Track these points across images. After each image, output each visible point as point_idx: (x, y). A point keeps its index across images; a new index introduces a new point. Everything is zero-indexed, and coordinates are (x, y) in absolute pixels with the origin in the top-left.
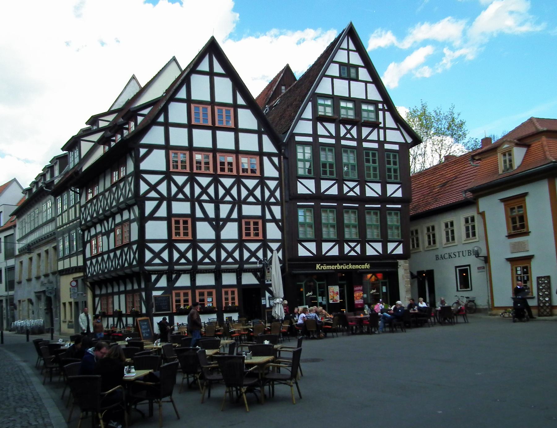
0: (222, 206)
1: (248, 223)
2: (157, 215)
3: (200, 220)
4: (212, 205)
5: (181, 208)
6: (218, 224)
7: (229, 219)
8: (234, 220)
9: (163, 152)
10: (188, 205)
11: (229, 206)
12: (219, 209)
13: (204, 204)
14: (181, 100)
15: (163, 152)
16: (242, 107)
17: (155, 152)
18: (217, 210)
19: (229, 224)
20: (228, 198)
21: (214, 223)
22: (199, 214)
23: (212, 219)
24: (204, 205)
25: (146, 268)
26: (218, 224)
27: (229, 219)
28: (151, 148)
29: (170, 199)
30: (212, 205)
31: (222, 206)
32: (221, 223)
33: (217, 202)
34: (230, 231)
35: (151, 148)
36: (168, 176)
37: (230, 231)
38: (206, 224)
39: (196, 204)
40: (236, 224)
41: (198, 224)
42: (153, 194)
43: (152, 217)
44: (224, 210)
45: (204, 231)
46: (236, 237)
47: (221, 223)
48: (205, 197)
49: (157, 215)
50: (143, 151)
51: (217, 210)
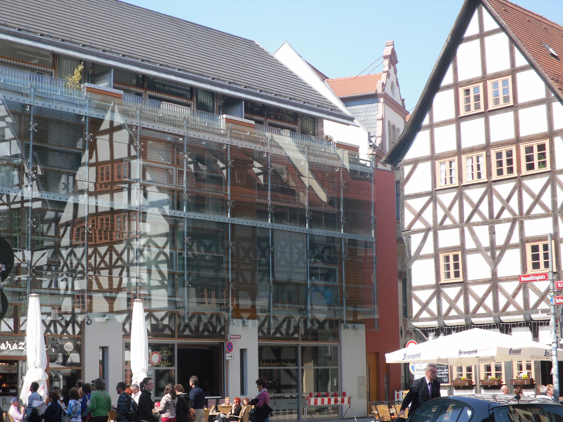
0: (497, 227)
1: (535, 249)
2: (422, 253)
3: (473, 251)
4: (486, 228)
5: (449, 238)
6: (494, 254)
7: (507, 246)
8: (515, 246)
9: (428, 164)
10: (457, 231)
11: (509, 225)
12: (494, 233)
13: (475, 228)
14: (448, 87)
15: (428, 164)
16: (523, 69)
17: (420, 165)
18: (492, 232)
19: (508, 252)
20: (506, 214)
21: (489, 254)
22: (470, 244)
23: (487, 249)
24: (475, 228)
25: (415, 324)
26: (494, 254)
27: (507, 246)
28: (415, 162)
29: (437, 228)
30: (486, 228)
31: (497, 227)
32: (498, 253)
33: (492, 221)
34: (510, 264)
35: (415, 162)
36: (432, 196)
37: (510, 264)
38: (479, 256)
39: (466, 229)
40: (517, 251)
41: (470, 258)
42: (419, 225)
43: (418, 256)
44: (502, 230)
45: (477, 267)
46: (518, 271)
47: (498, 253)
48: (476, 218)
49: (422, 253)
50: (407, 169)
51: (492, 232)
